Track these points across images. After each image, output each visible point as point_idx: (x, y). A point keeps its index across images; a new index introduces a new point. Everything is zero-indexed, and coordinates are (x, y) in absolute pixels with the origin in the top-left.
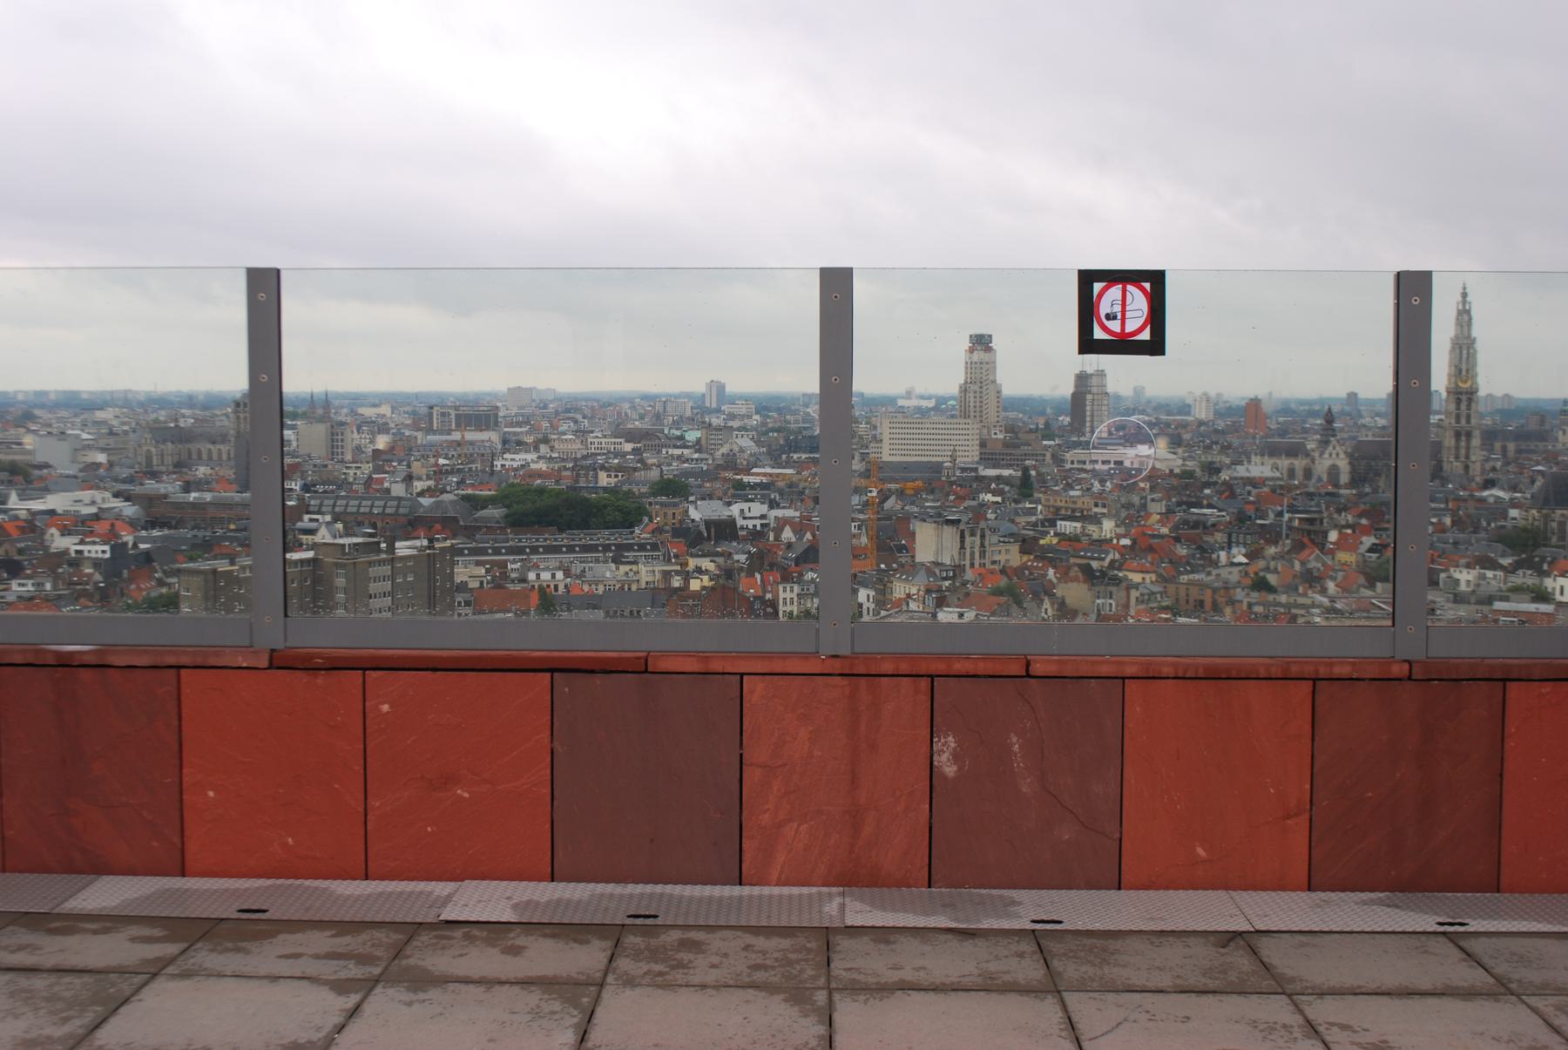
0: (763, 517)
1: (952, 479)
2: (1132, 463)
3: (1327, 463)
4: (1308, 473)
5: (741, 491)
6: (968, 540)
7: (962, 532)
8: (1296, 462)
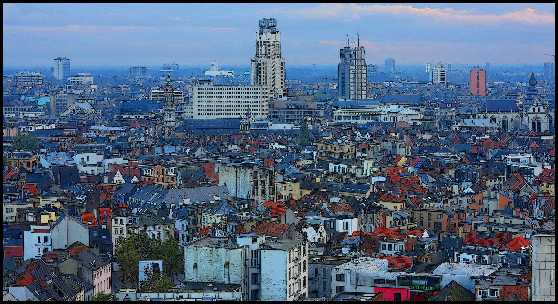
0: (99, 164)
1: (247, 132)
2: (386, 118)
3: (532, 116)
4: (517, 123)
6: (260, 179)
7: (256, 173)
8: (509, 116)
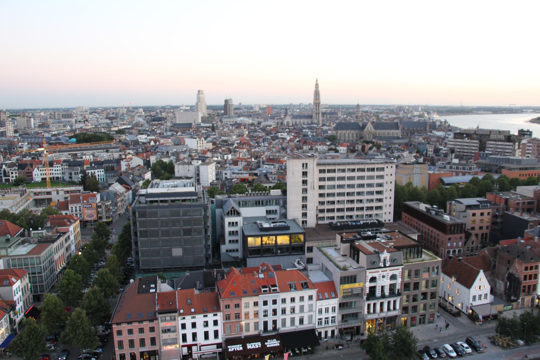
0: (146, 139)
5: (140, 133)
6: (199, 143)
